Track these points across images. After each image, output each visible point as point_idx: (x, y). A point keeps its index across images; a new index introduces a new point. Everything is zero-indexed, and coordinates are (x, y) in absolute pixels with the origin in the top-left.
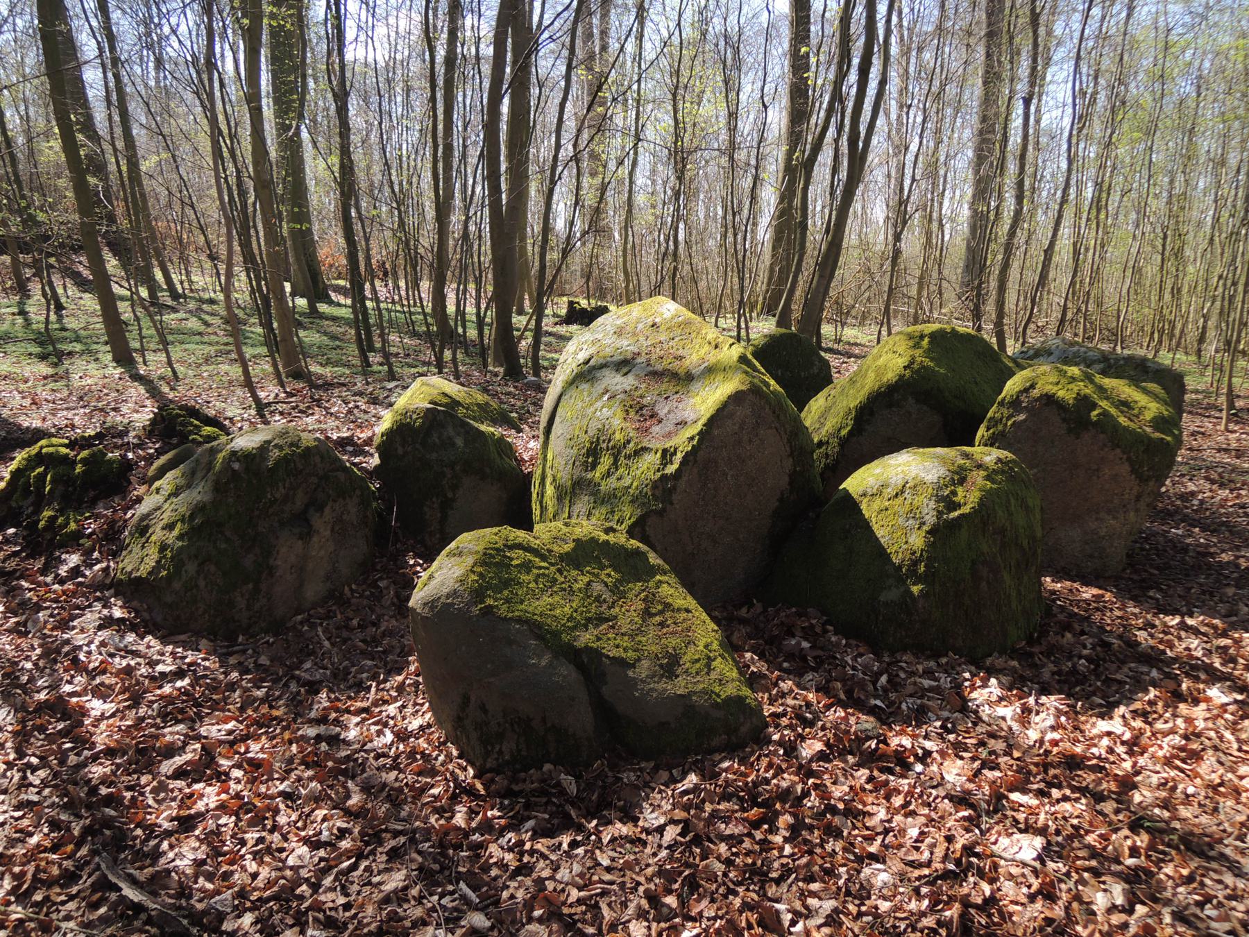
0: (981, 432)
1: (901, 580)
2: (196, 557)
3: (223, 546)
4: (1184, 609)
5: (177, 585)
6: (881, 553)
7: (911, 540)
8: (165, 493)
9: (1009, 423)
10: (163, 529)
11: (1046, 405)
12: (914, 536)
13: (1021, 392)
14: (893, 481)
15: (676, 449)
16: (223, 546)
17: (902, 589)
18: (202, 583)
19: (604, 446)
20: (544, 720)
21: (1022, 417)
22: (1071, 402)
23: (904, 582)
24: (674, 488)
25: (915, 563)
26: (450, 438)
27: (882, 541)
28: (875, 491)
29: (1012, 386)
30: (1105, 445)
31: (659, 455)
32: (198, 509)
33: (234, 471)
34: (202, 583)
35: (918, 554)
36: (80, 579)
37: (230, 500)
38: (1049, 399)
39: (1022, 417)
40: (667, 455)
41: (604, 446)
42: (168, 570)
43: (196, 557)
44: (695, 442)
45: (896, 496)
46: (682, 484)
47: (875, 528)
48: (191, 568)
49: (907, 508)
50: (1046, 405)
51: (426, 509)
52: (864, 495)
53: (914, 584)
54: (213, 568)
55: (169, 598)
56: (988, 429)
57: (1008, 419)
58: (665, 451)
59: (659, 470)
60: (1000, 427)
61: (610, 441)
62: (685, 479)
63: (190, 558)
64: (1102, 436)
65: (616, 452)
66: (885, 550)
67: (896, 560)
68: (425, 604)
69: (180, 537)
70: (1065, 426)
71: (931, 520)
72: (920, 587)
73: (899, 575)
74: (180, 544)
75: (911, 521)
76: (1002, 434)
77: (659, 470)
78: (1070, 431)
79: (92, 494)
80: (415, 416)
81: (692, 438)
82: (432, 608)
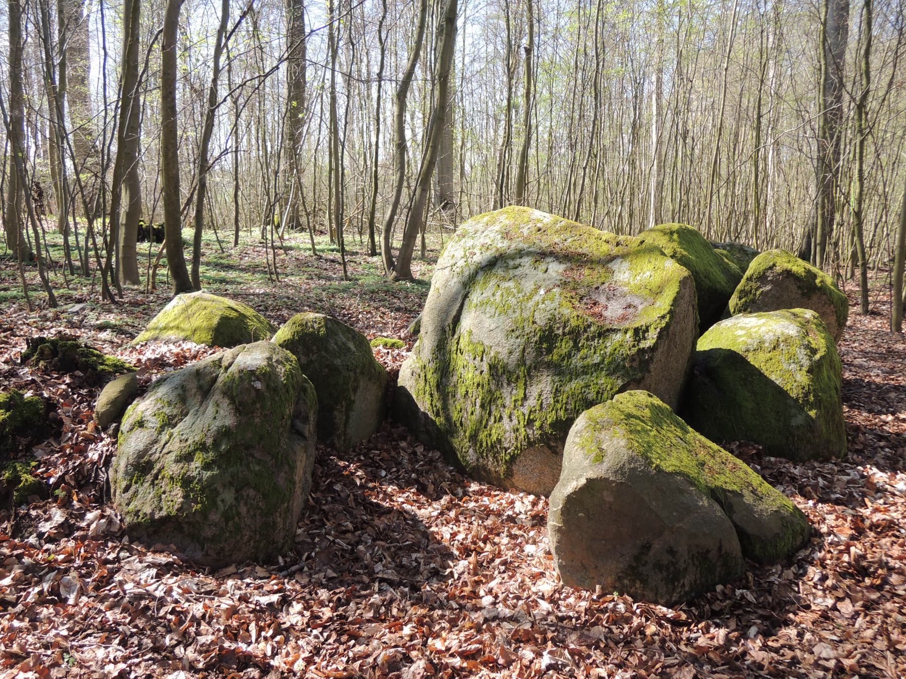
0: (733, 302)
1: (801, 409)
2: (231, 484)
3: (257, 468)
4: (884, 410)
5: (215, 517)
6: (781, 393)
7: (798, 379)
8: (154, 423)
9: (758, 293)
10: (177, 461)
11: (787, 277)
12: (799, 376)
13: (767, 269)
14: (767, 337)
15: (647, 327)
16: (257, 468)
17: (804, 415)
18: (243, 510)
19: (560, 332)
20: (720, 549)
21: (768, 288)
22: (803, 274)
23: (802, 409)
24: (651, 359)
25: (806, 395)
26: (344, 344)
27: (777, 382)
28: (755, 347)
29: (754, 266)
30: (825, 303)
31: (629, 334)
32: (224, 434)
33: (257, 391)
34: (243, 510)
35: (807, 389)
36: (77, 534)
37: (257, 420)
38: (788, 273)
39: (768, 288)
40: (639, 333)
41: (560, 332)
42: (202, 502)
43: (231, 484)
44: (667, 319)
45: (774, 348)
46: (658, 355)
47: (767, 374)
48: (228, 496)
49: (787, 357)
50: (787, 277)
51: (336, 413)
52: (748, 351)
53: (810, 410)
54: (252, 493)
55: (208, 532)
56: (740, 298)
57: (757, 290)
58: (636, 331)
59: (634, 346)
60: (751, 297)
61: (565, 327)
62: (660, 350)
63: (224, 486)
64: (824, 297)
65: (575, 334)
66: (782, 389)
67: (793, 395)
68: (616, 472)
69: (207, 466)
70: (800, 292)
71: (806, 363)
72: (814, 411)
73: (799, 406)
74: (209, 473)
75: (793, 366)
76: (753, 301)
77: (634, 346)
78: (803, 294)
79: (24, 441)
80: (316, 326)
81: (663, 317)
82: (623, 474)
